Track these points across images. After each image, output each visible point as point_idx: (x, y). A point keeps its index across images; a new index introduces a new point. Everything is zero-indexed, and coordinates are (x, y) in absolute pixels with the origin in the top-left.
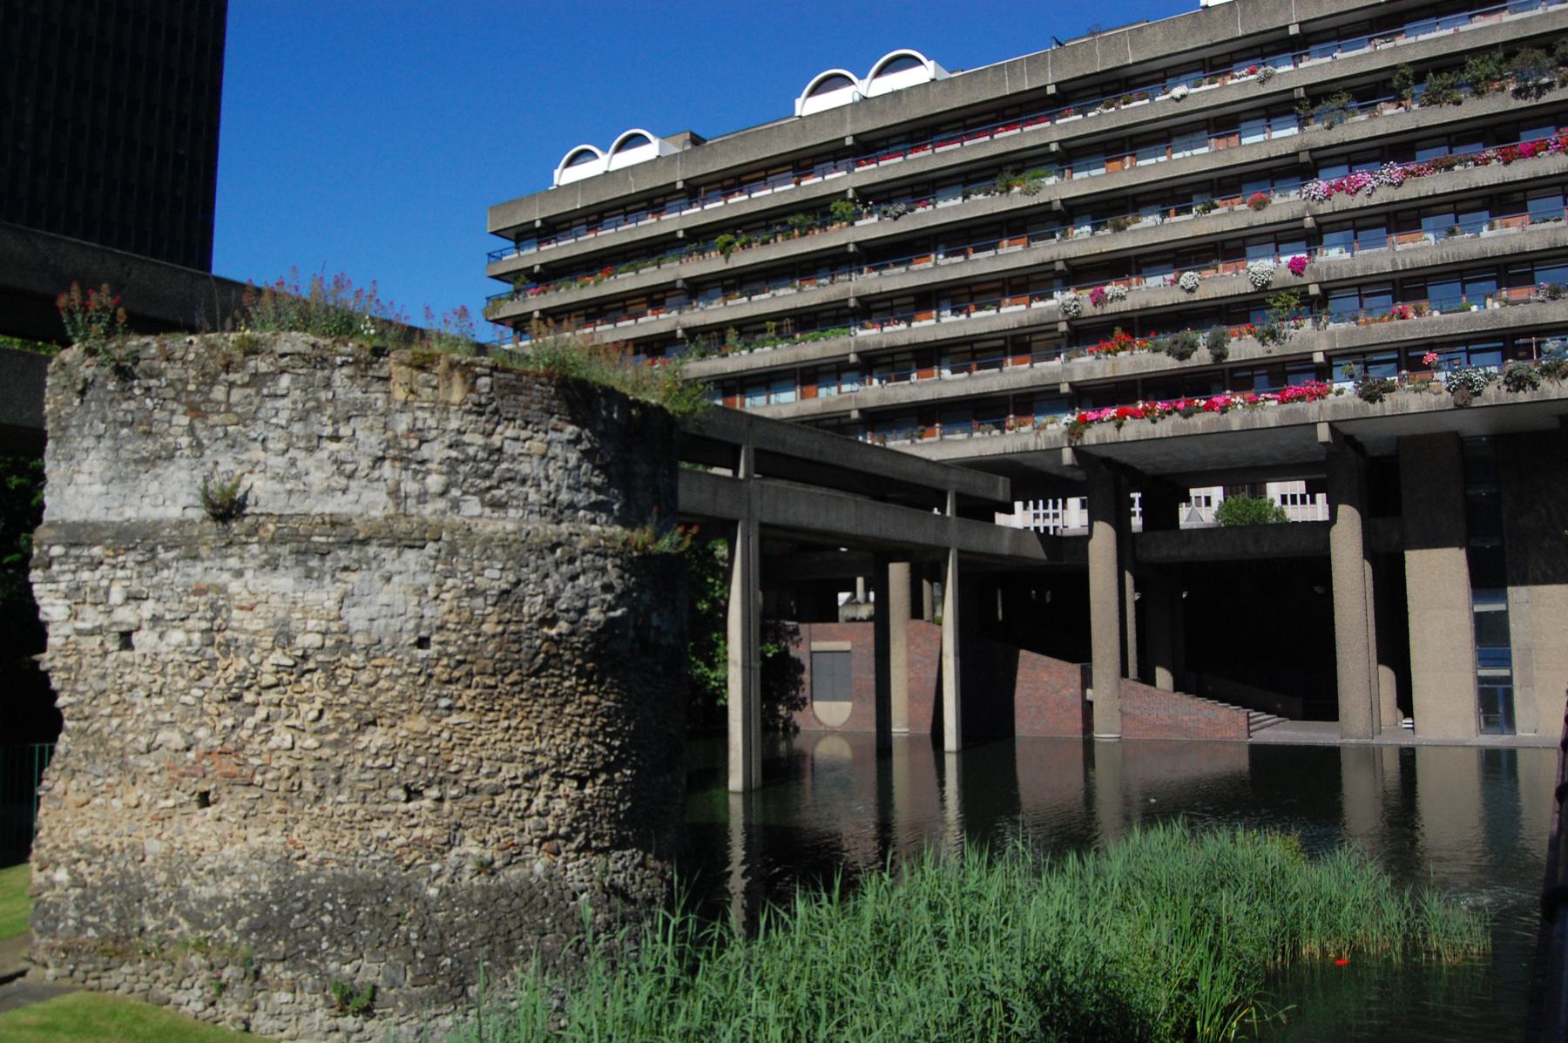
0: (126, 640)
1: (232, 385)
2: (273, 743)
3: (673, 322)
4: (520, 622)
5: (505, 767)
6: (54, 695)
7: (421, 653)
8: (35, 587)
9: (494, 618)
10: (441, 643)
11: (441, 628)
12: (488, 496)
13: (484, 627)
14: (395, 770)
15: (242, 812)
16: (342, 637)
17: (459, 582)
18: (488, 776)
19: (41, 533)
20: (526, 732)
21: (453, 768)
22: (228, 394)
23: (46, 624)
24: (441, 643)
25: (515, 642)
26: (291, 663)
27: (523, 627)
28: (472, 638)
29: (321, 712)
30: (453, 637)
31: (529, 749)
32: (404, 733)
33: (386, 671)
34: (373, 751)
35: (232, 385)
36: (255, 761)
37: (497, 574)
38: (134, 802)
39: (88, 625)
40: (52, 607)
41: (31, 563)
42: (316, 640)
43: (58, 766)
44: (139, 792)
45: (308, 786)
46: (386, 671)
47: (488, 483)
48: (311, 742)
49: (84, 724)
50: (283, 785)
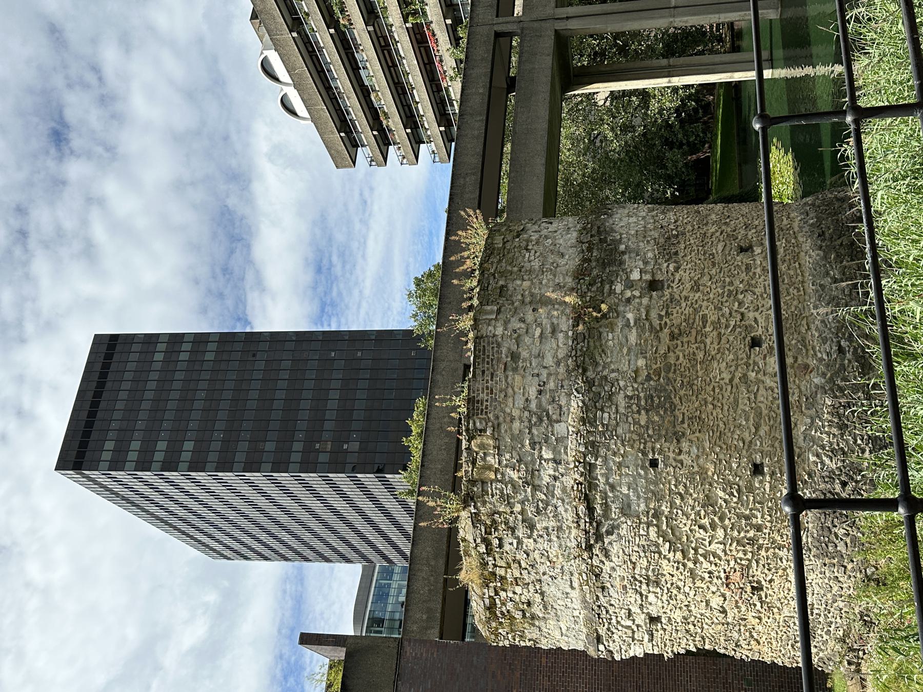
0: (654, 620)
1: (495, 566)
2: (722, 554)
3: (401, 30)
4: (639, 398)
5: (741, 406)
6: (688, 652)
7: (661, 465)
8: (624, 657)
9: (636, 416)
10: (654, 454)
11: (644, 454)
12: (554, 417)
13: (643, 423)
14: (741, 483)
15: (766, 571)
16: (650, 514)
17: (613, 441)
18: (747, 420)
19: (592, 652)
20: (717, 390)
21: (742, 445)
22: (501, 567)
23: (646, 654)
24: (654, 454)
25: (652, 401)
26: (668, 544)
27: (642, 395)
28: (650, 432)
29: (700, 527)
30: (649, 445)
31: (729, 388)
32: (716, 477)
33: (673, 487)
34: (727, 497)
35: (495, 566)
36: (732, 563)
37: (606, 415)
38: (758, 621)
39: (646, 637)
40: (637, 651)
41: (610, 659)
42: (653, 531)
43: (733, 653)
44: (750, 617)
45: (751, 534)
46: (673, 487)
47: (545, 418)
48: (720, 533)
49: (707, 641)
50: (749, 548)
